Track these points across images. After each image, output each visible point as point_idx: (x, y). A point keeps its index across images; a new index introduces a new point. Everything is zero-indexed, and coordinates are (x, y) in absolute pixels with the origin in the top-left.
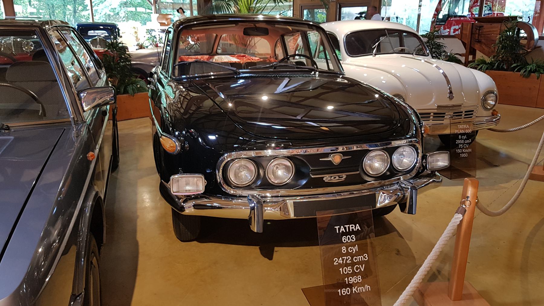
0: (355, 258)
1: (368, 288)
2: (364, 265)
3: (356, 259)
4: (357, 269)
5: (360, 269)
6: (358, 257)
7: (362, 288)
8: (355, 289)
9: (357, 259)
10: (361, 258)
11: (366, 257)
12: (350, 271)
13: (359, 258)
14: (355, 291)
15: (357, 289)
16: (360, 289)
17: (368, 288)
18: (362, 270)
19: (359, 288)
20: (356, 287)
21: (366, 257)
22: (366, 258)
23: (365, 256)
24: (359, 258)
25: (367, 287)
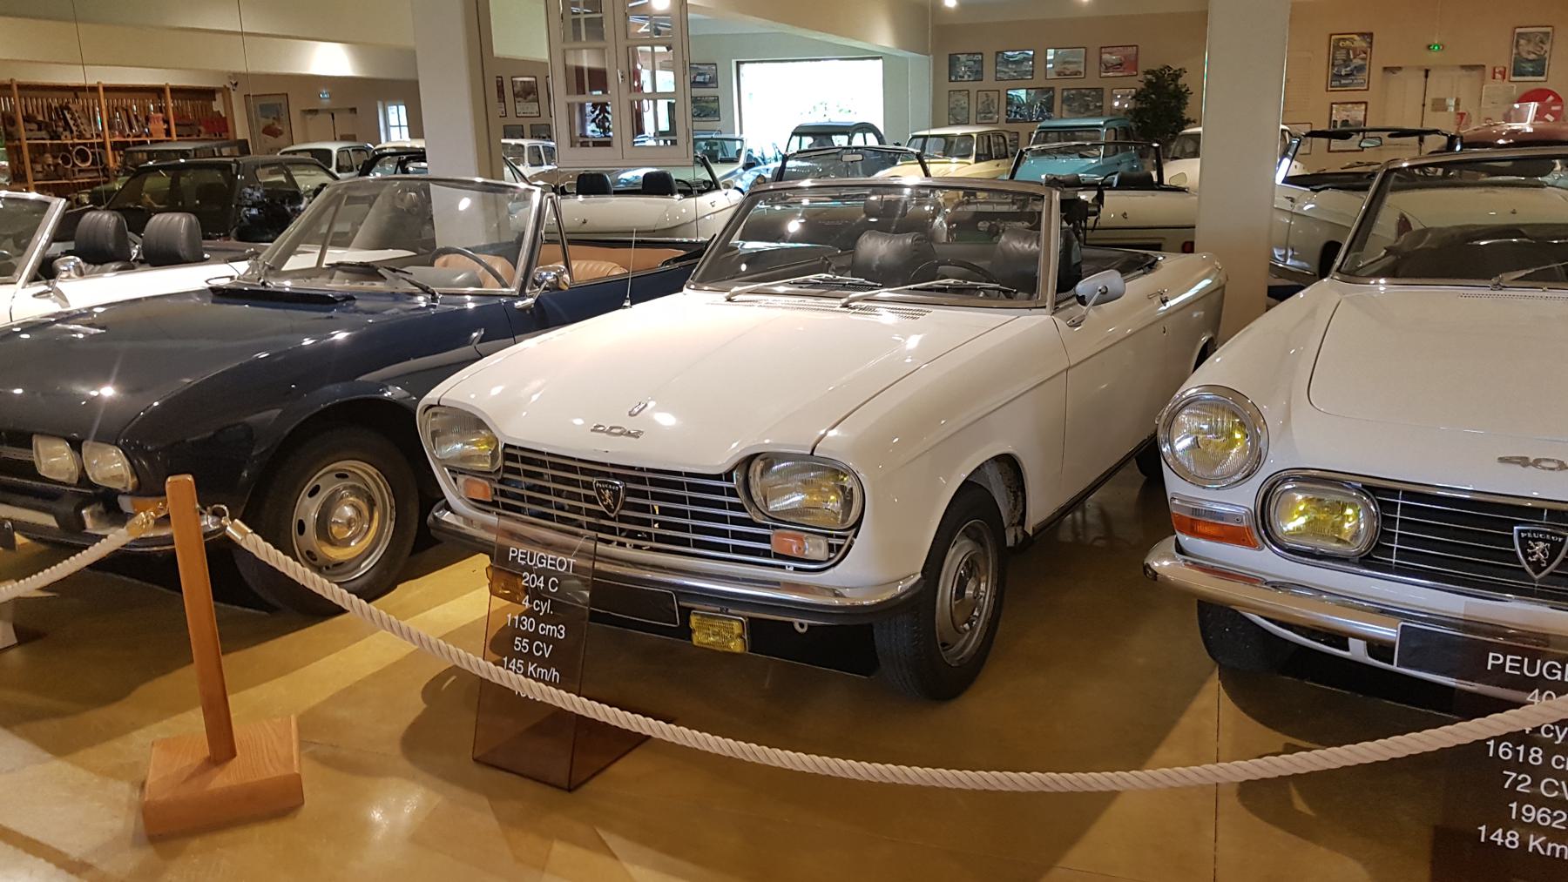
1: (556, 675)
3: (543, 629)
6: (548, 627)
7: (544, 672)
9: (545, 630)
10: (554, 630)
11: (562, 632)
13: (549, 629)
14: (531, 672)
15: (535, 669)
17: (556, 675)
19: (539, 670)
20: (535, 665)
21: (562, 632)
22: (561, 635)
23: (562, 629)
24: (549, 629)
25: (554, 673)
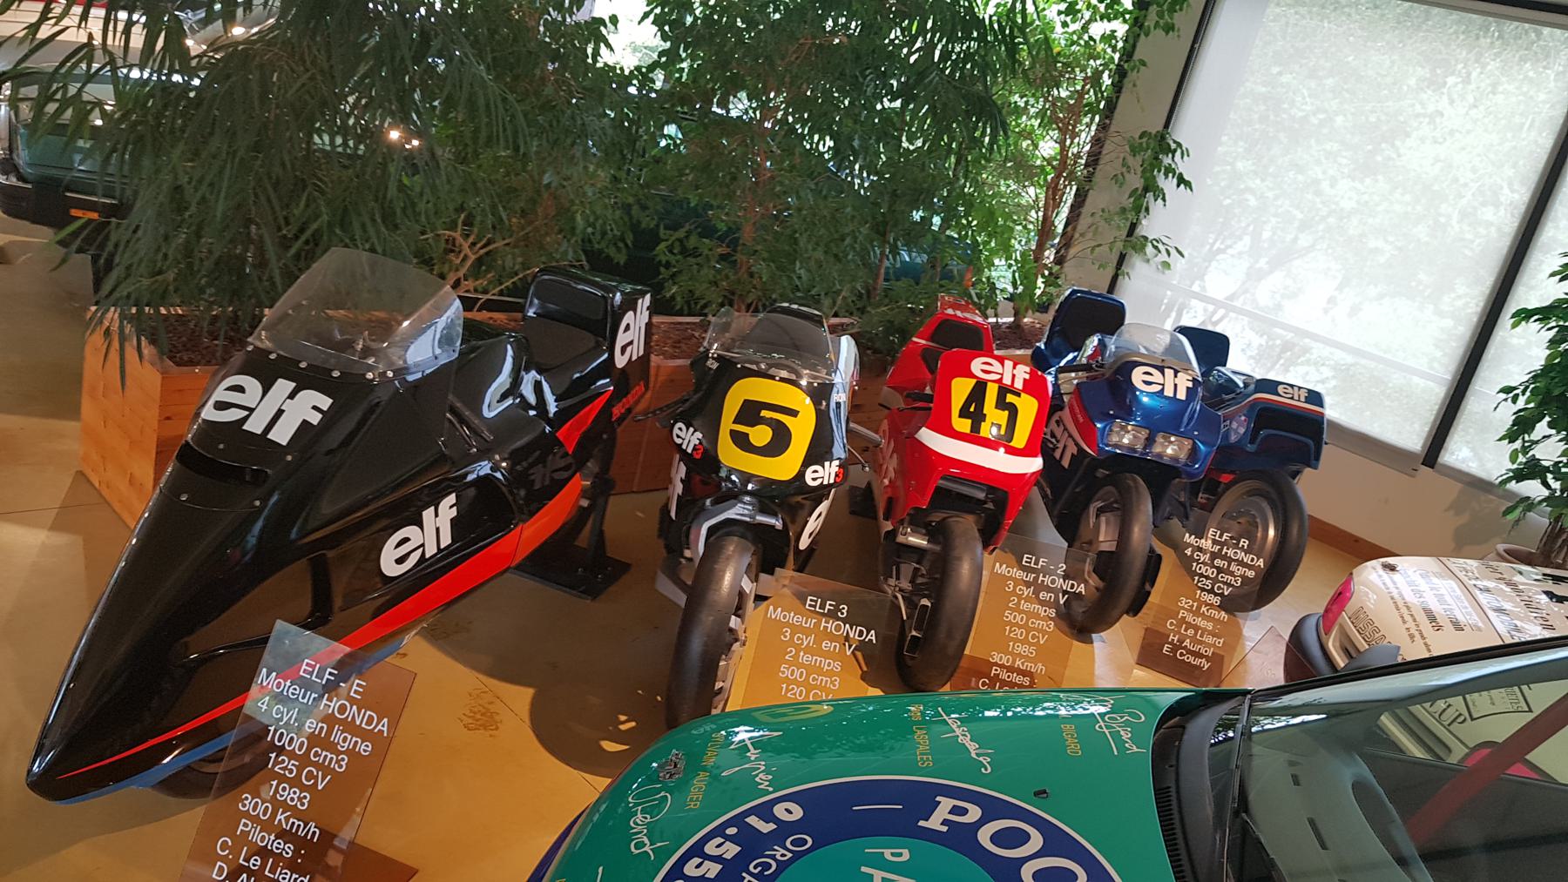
0: (317, 751)
1: (314, 833)
2: (329, 777)
3: (316, 754)
4: (310, 776)
5: (316, 784)
6: (324, 753)
7: (299, 826)
8: (282, 817)
10: (332, 758)
12: (291, 771)
13: (326, 756)
15: (287, 819)
16: (293, 823)
17: (314, 833)
18: (320, 788)
19: (291, 820)
21: (343, 763)
22: (340, 767)
24: (326, 756)
25: (312, 830)
